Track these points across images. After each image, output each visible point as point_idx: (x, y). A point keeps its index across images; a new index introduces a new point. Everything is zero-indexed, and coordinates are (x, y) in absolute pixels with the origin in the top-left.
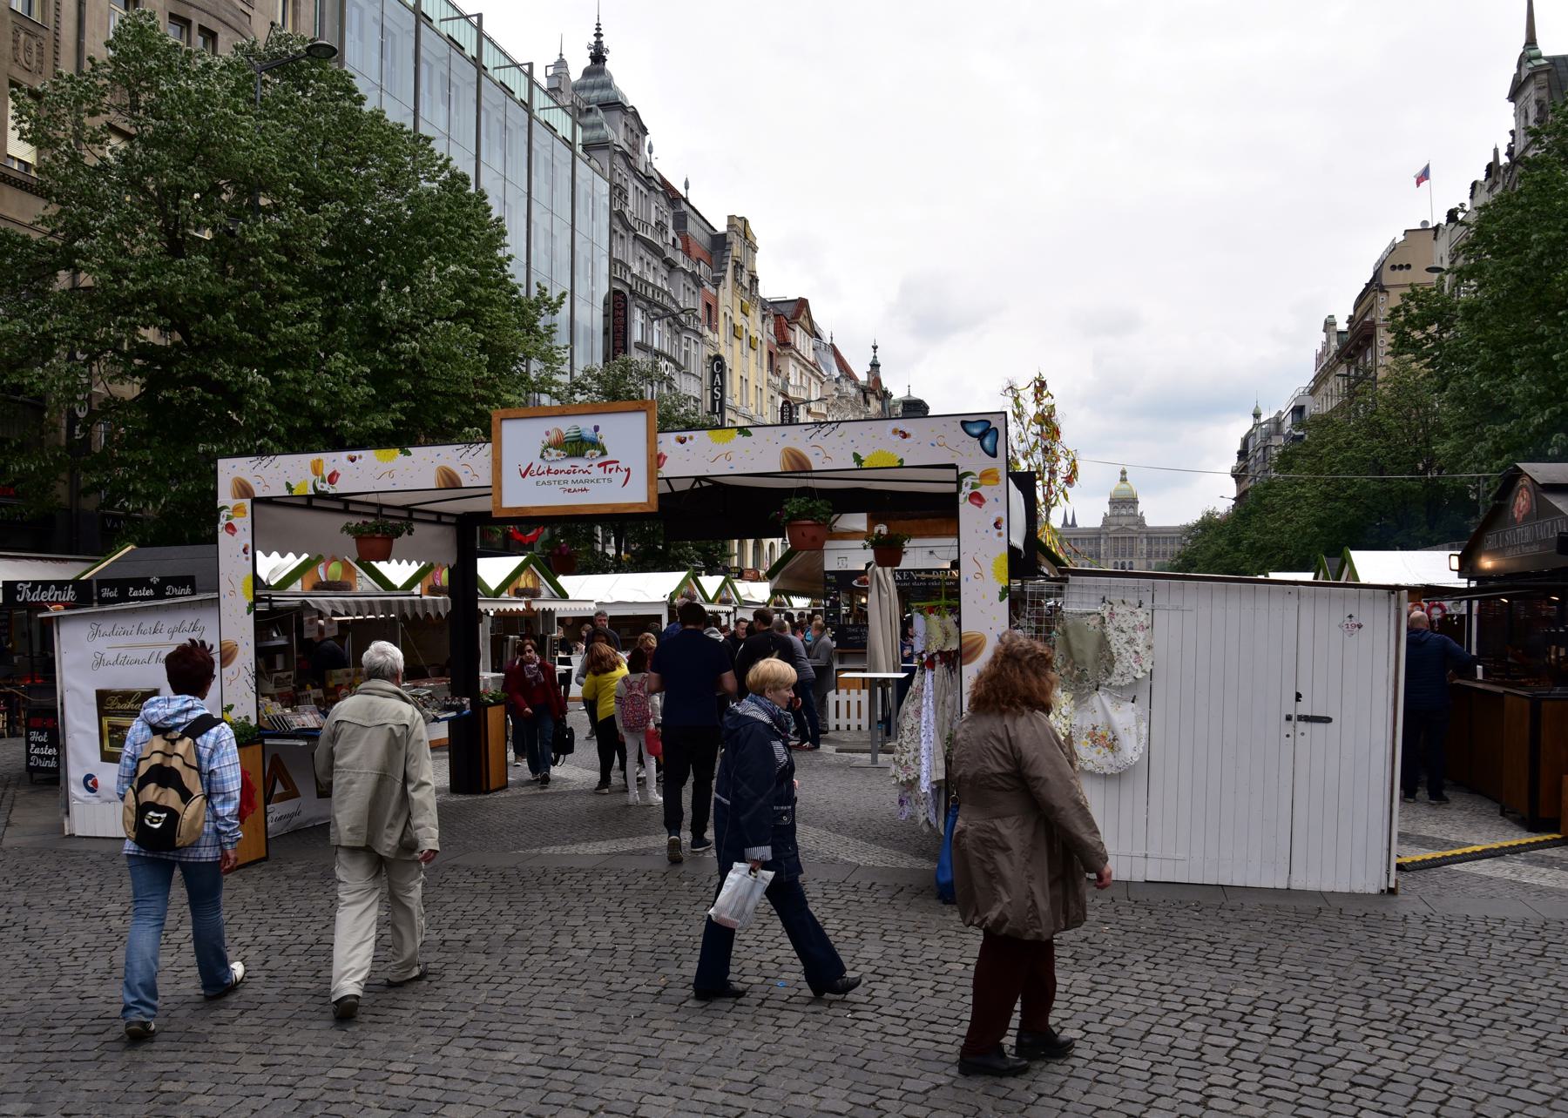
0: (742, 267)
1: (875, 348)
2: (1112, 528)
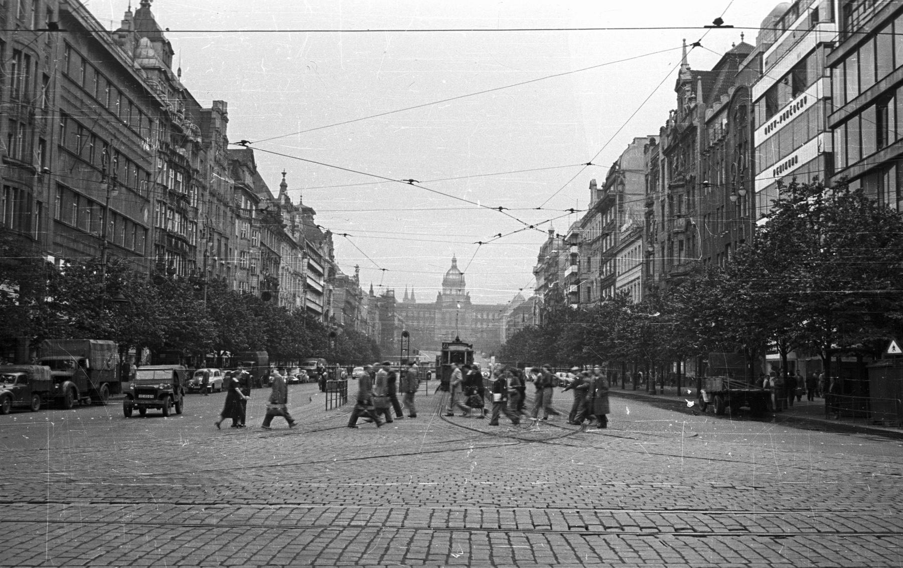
0: (220, 135)
1: (284, 174)
2: (444, 305)
